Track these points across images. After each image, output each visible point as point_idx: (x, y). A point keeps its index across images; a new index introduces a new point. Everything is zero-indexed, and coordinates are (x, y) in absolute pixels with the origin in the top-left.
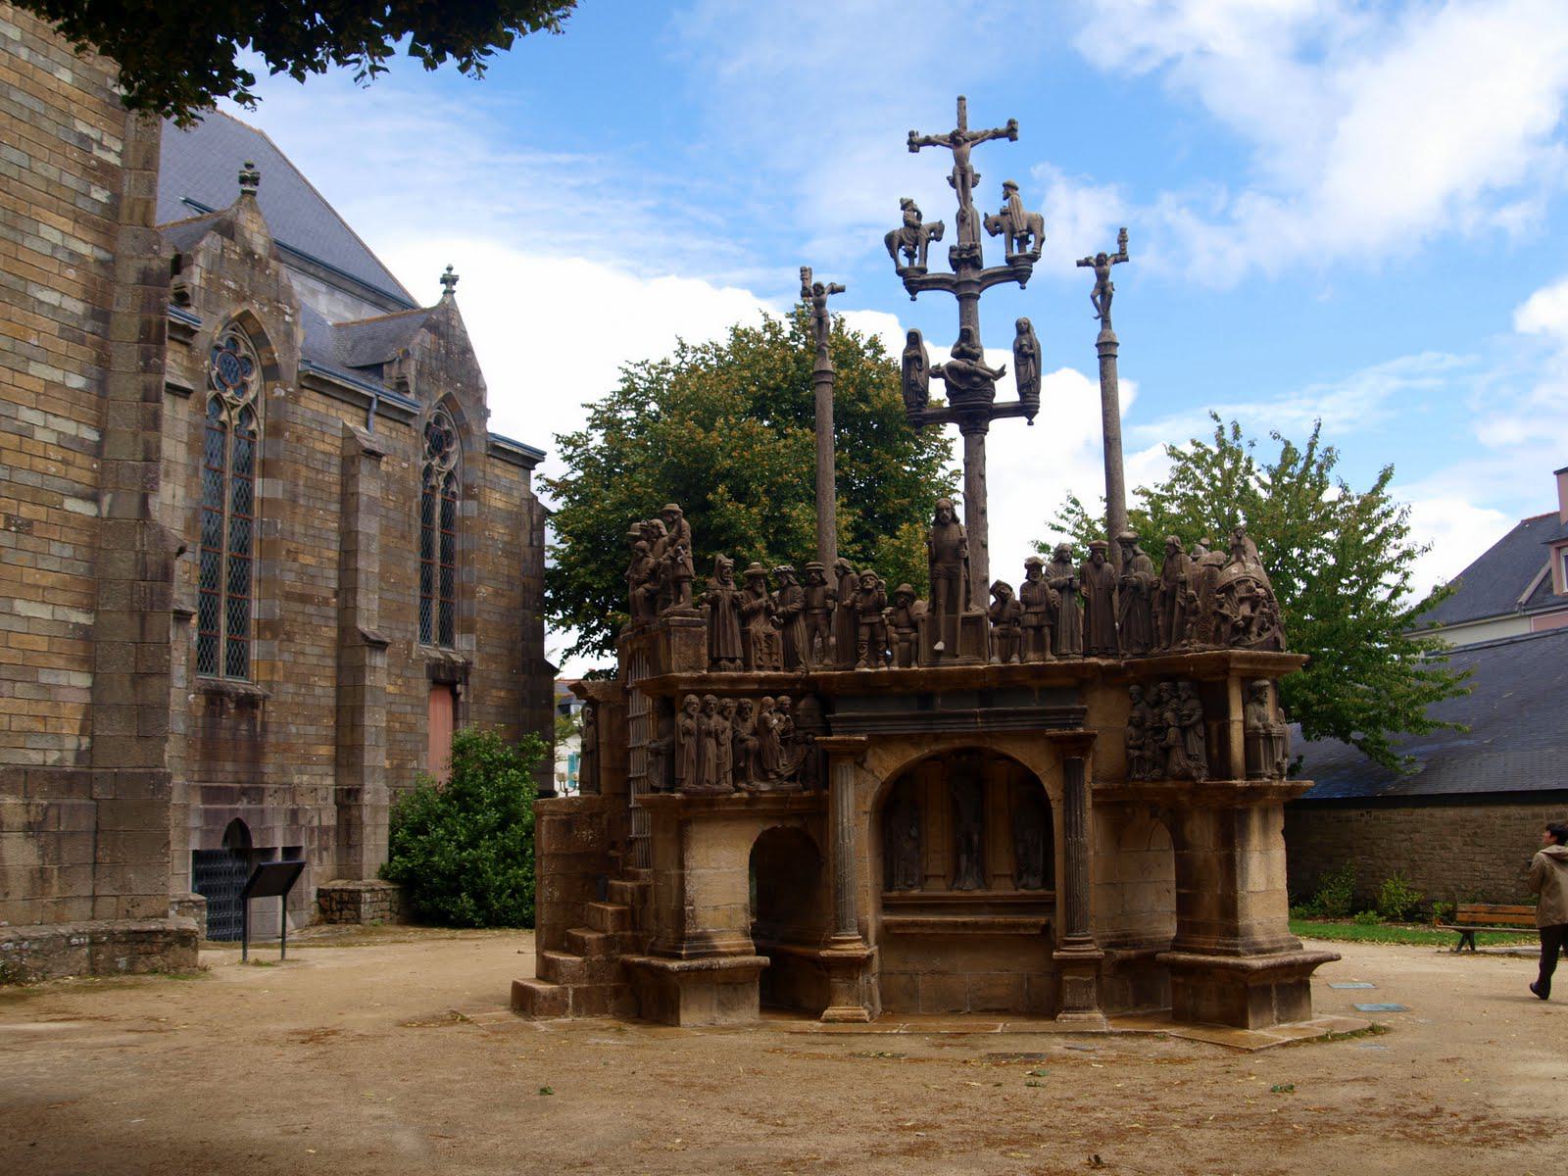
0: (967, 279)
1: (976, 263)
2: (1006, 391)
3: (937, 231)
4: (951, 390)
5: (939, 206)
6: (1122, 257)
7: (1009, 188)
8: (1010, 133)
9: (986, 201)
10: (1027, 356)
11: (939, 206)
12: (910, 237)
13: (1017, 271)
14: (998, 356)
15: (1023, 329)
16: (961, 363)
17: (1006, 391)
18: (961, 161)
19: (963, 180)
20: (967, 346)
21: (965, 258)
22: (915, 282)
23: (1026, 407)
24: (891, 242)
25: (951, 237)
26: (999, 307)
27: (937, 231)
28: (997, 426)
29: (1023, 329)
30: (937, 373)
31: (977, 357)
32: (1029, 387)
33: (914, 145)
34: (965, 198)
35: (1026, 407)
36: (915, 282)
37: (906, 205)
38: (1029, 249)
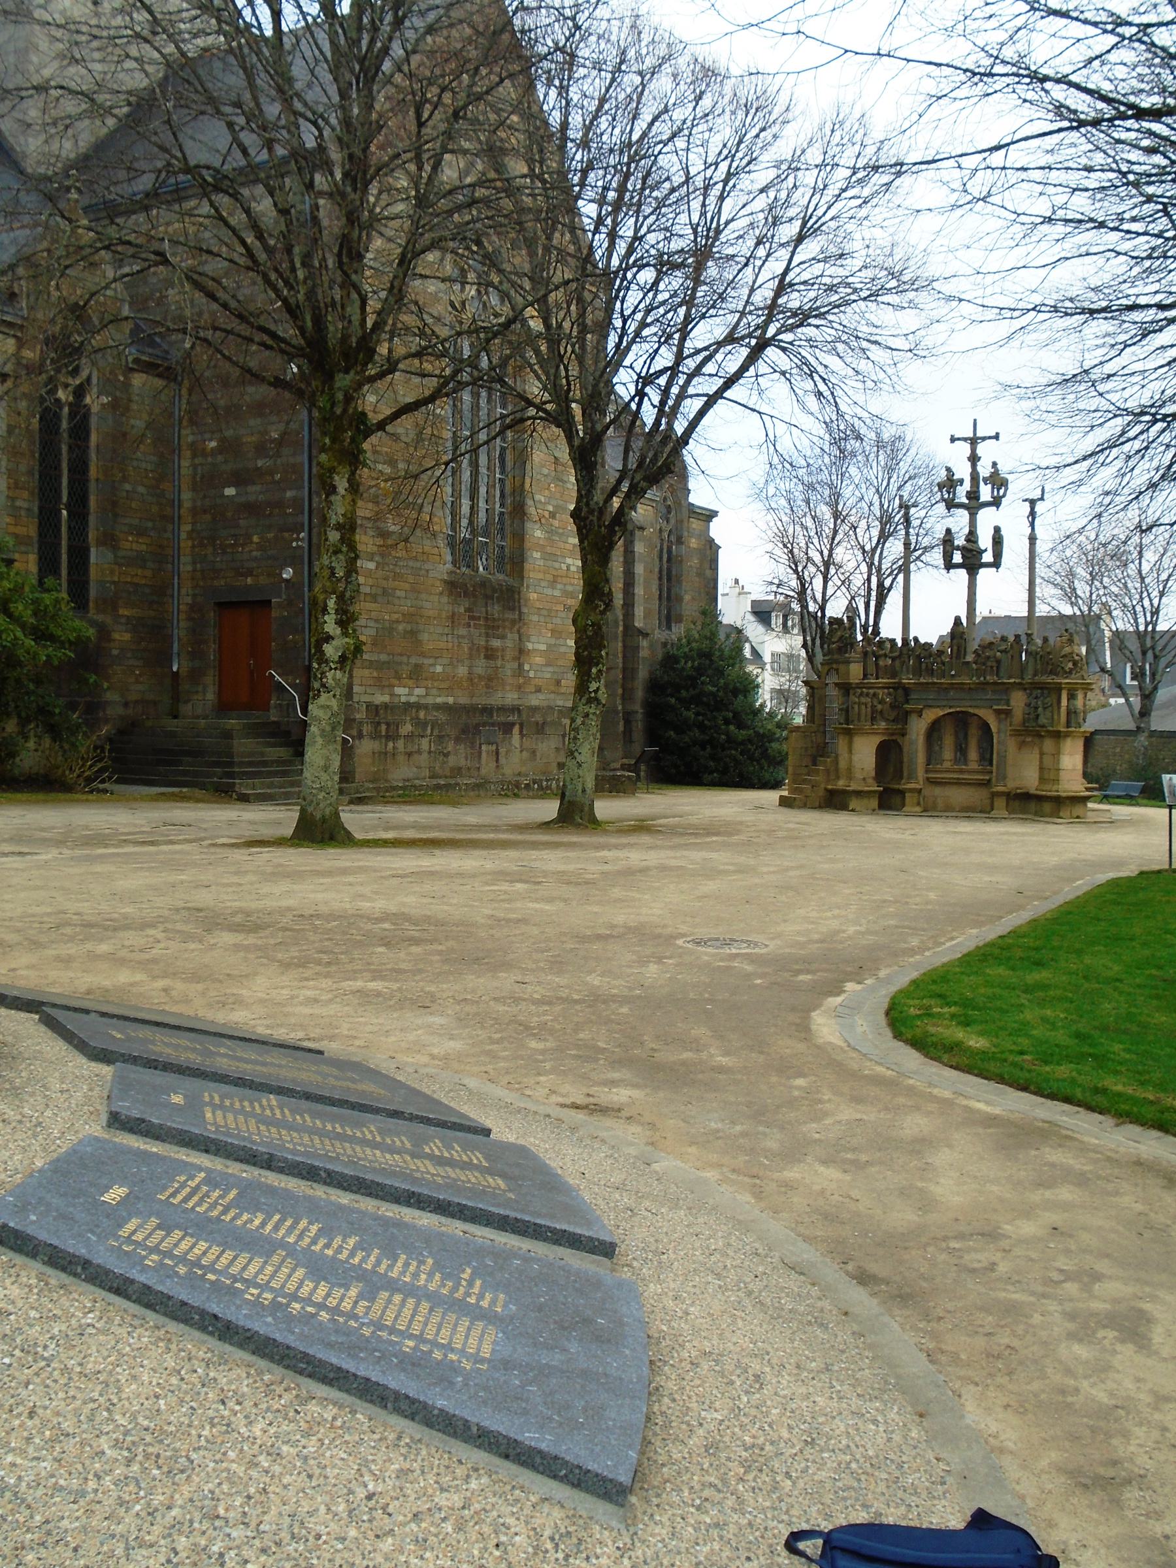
0: (974, 504)
1: (978, 498)
2: (988, 557)
3: (961, 481)
4: (963, 557)
5: (963, 471)
6: (1042, 499)
7: (994, 464)
8: (997, 437)
9: (984, 470)
10: (998, 541)
11: (963, 471)
12: (950, 483)
13: (996, 502)
14: (985, 541)
15: (997, 530)
16: (969, 546)
17: (988, 557)
18: (973, 450)
19: (974, 459)
20: (972, 536)
21: (973, 495)
22: (951, 505)
23: (996, 564)
24: (941, 486)
25: (967, 486)
26: (987, 519)
27: (961, 481)
28: (982, 571)
29: (997, 530)
30: (958, 548)
31: (976, 542)
32: (998, 555)
33: (953, 440)
34: (974, 466)
35: (996, 564)
36: (951, 505)
37: (948, 469)
38: (1002, 492)
